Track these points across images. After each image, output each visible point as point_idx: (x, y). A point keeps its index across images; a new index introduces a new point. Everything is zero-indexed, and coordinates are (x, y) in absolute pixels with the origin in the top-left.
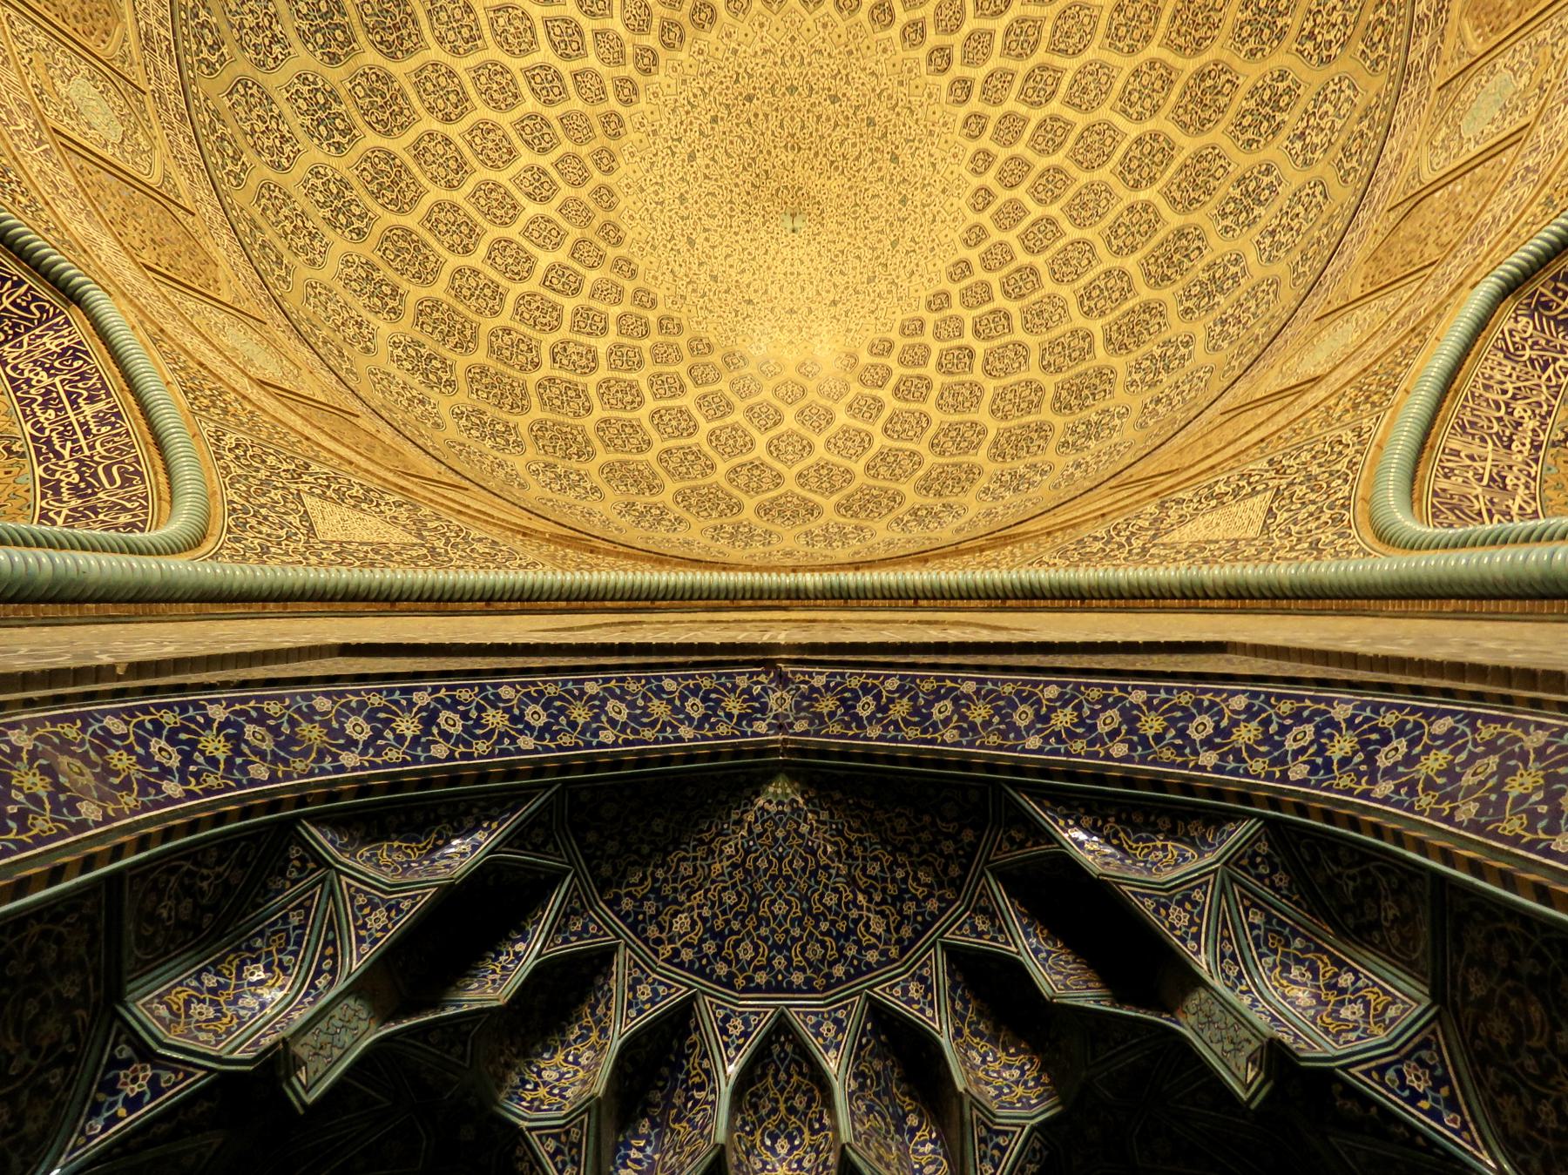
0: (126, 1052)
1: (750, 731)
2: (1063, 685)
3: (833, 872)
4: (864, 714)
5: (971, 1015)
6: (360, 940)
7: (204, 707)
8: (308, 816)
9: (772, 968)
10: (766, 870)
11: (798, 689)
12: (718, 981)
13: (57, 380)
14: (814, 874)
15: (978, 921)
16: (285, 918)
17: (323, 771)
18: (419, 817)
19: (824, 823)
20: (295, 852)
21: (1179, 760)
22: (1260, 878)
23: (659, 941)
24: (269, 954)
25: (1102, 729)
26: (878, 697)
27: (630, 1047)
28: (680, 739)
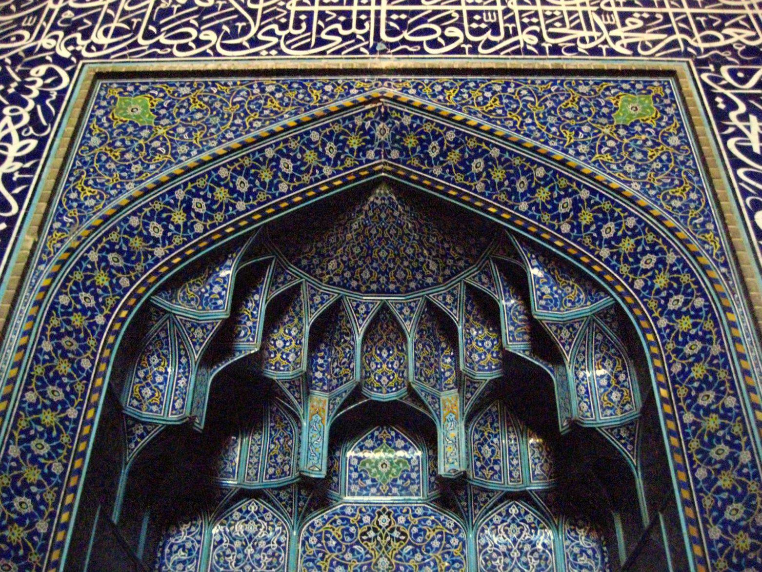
1: (364, 159)
2: (547, 169)
3: (412, 238)
4: (433, 155)
5: (475, 312)
6: (194, 344)
8: (152, 294)
9: (379, 282)
10: (375, 235)
11: (393, 123)
12: (353, 289)
14: (401, 238)
15: (483, 277)
16: (158, 335)
17: (151, 266)
19: (407, 212)
20: (152, 310)
21: (592, 247)
22: (606, 323)
23: (322, 275)
24: (157, 350)
25: (561, 210)
26: (441, 144)
27: (314, 327)
28: (324, 177)
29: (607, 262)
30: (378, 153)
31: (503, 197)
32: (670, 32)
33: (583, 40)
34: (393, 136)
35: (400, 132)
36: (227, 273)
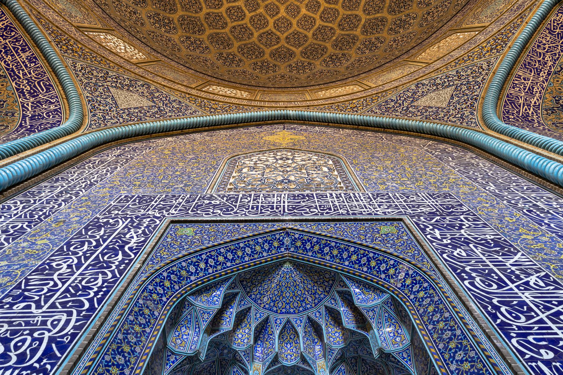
0: (170, 354)
2: (355, 248)
4: (308, 248)
5: (330, 320)
6: (203, 321)
7: (162, 274)
8: (188, 295)
12: (274, 312)
13: (7, 41)
14: (295, 286)
15: (332, 301)
18: (208, 288)
20: (186, 303)
23: (261, 304)
26: (311, 243)
28: (263, 257)
29: (384, 279)
30: (285, 249)
31: (338, 261)
32: (399, 209)
33: (364, 211)
34: (291, 242)
35: (295, 240)
36: (219, 295)
